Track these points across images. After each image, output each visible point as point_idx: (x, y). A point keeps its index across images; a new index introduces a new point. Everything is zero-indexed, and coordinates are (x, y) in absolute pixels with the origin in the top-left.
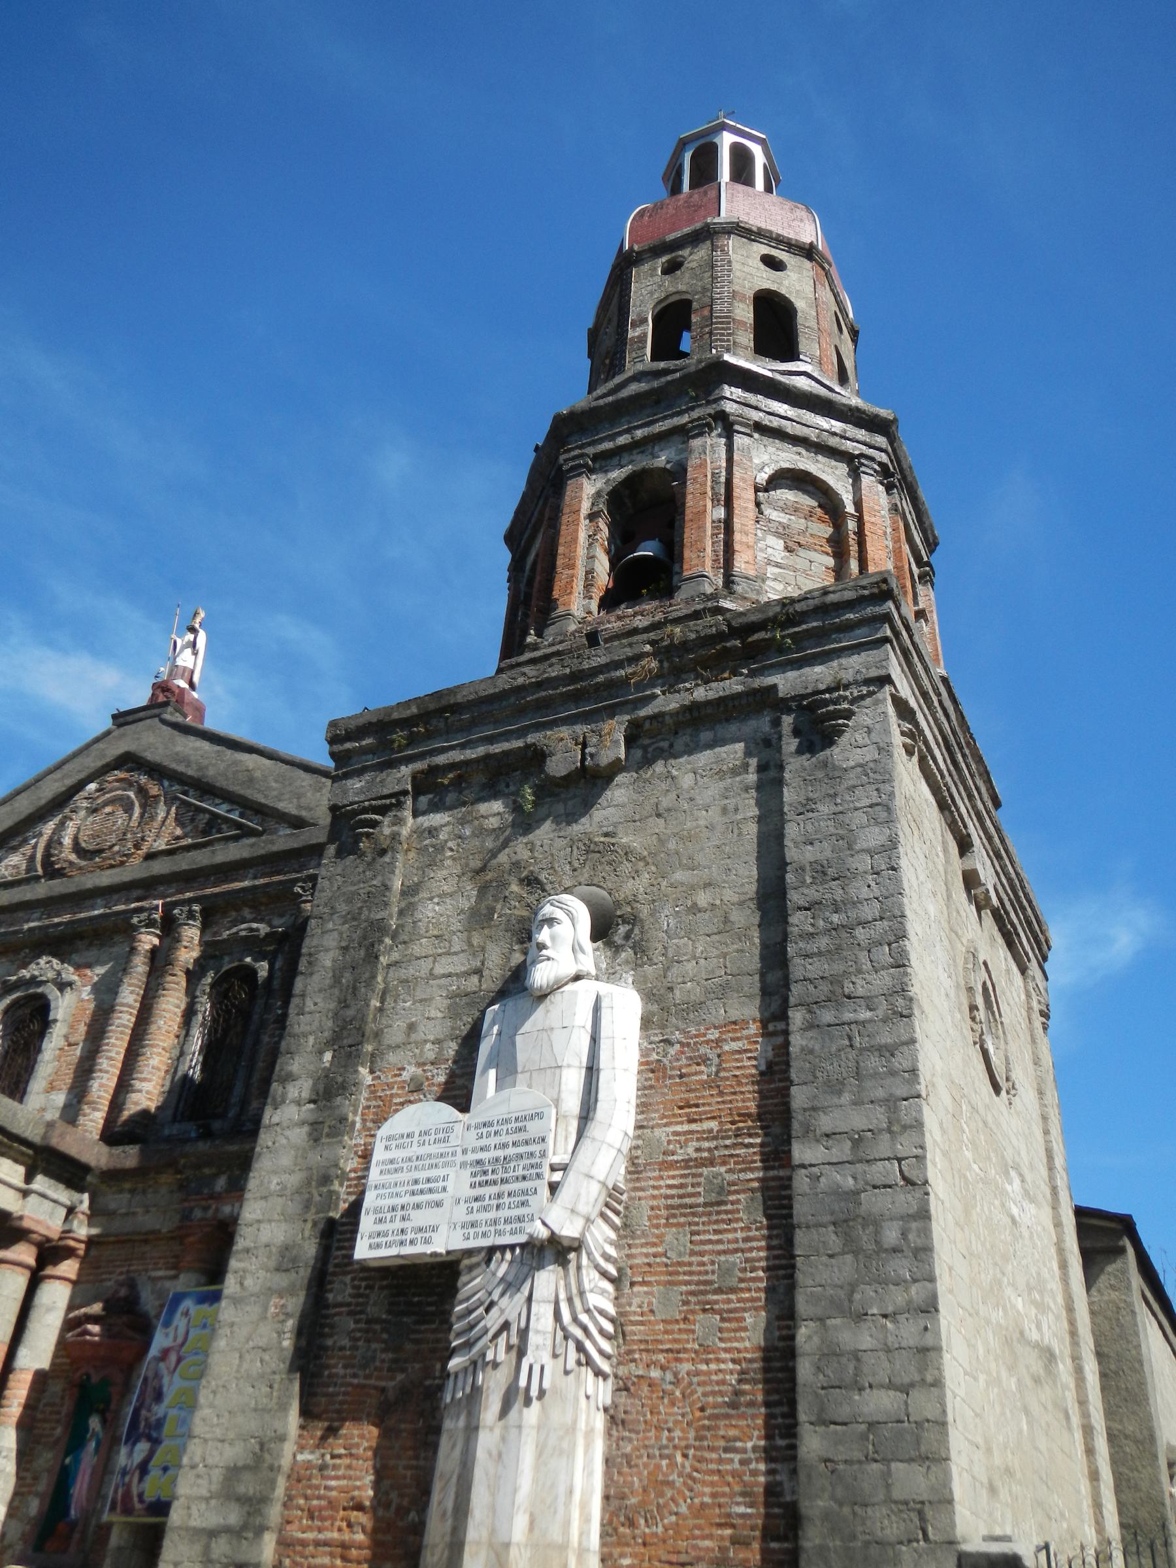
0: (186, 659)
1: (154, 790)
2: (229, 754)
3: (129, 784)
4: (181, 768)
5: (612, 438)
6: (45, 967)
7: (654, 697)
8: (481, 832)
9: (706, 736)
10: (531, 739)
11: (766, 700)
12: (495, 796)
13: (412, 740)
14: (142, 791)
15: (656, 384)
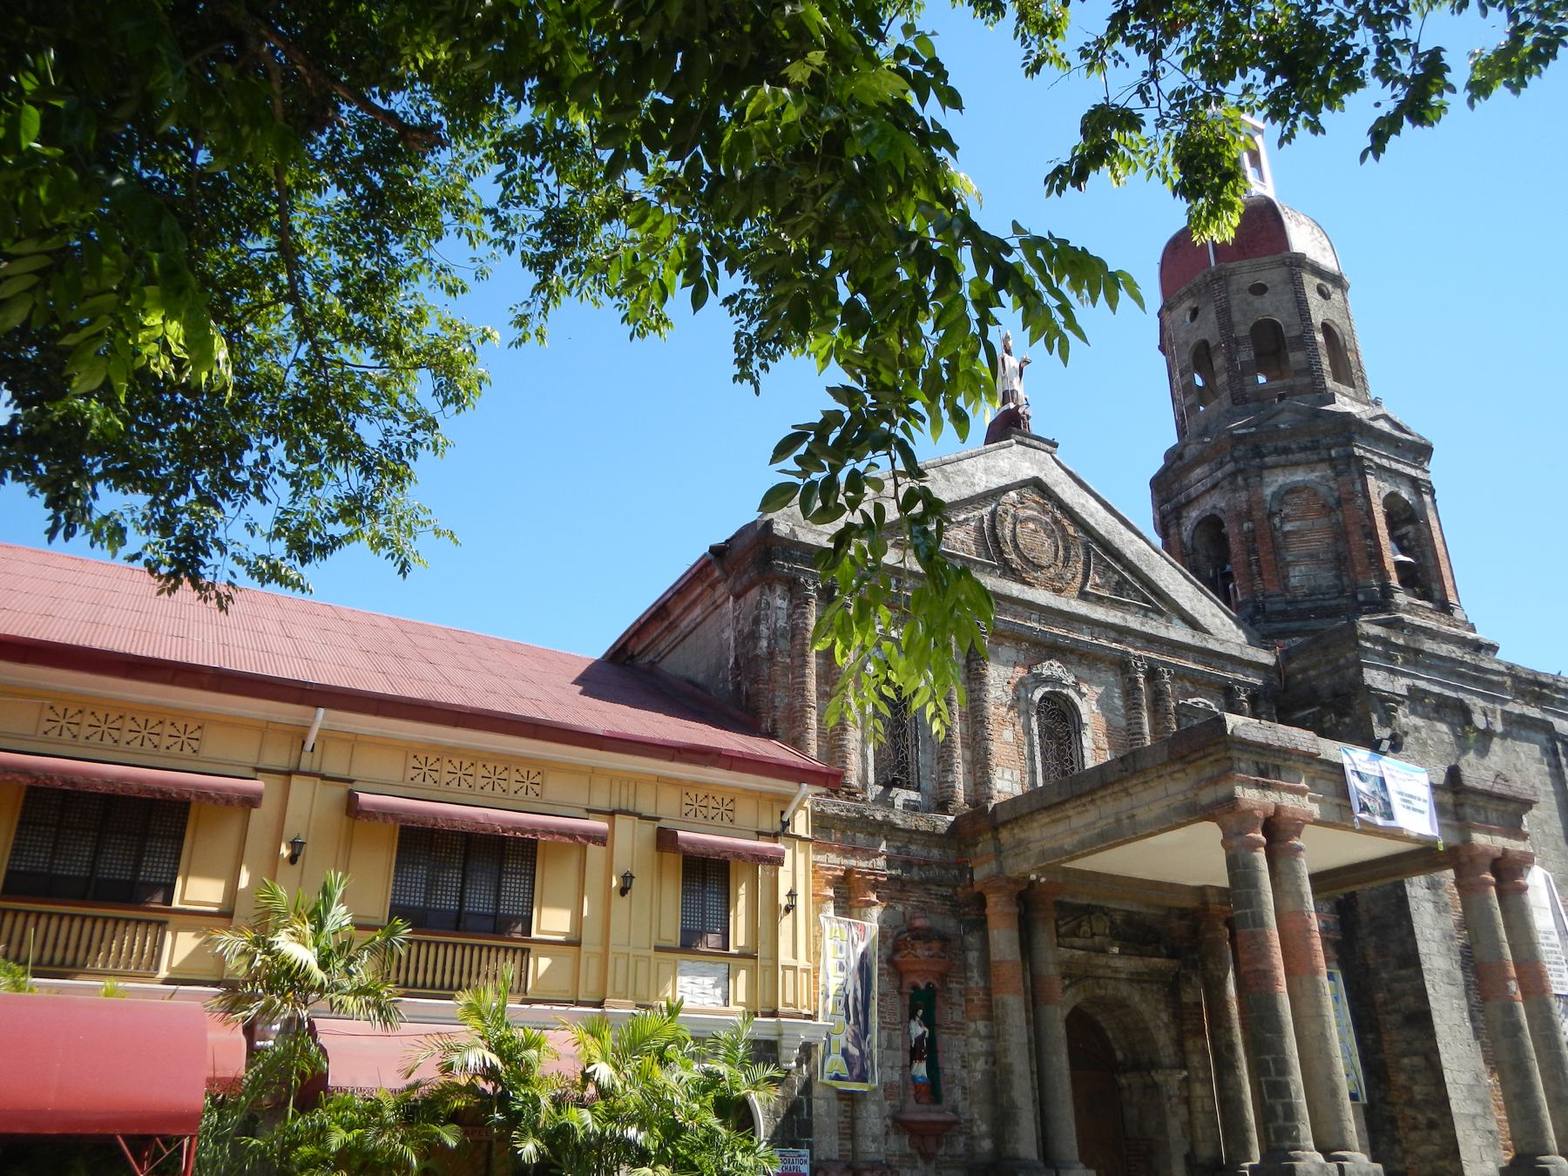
0: (1017, 386)
1: (1071, 530)
2: (1122, 527)
3: (1046, 512)
4: (1091, 522)
5: (1381, 456)
6: (1052, 668)
7: (1507, 701)
8: (1443, 741)
9: (1523, 733)
10: (1461, 695)
11: (1547, 728)
12: (1441, 720)
13: (1406, 662)
14: (1056, 521)
15: (1397, 433)
